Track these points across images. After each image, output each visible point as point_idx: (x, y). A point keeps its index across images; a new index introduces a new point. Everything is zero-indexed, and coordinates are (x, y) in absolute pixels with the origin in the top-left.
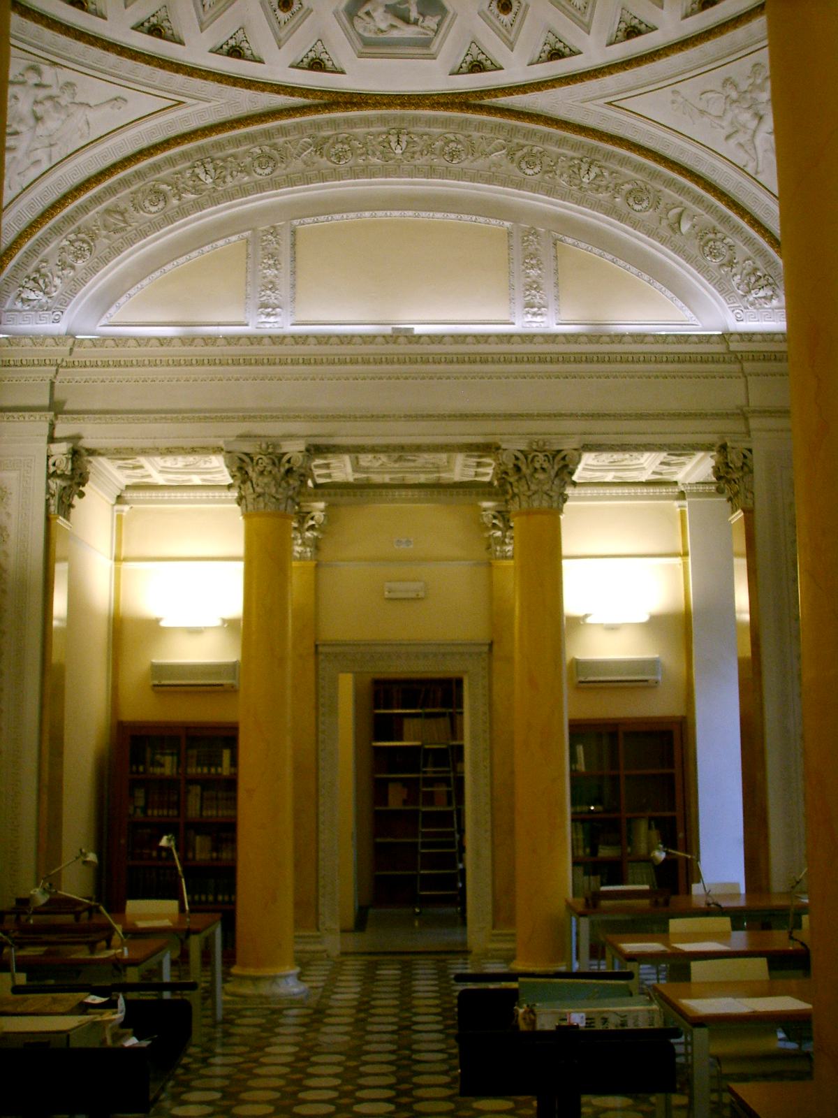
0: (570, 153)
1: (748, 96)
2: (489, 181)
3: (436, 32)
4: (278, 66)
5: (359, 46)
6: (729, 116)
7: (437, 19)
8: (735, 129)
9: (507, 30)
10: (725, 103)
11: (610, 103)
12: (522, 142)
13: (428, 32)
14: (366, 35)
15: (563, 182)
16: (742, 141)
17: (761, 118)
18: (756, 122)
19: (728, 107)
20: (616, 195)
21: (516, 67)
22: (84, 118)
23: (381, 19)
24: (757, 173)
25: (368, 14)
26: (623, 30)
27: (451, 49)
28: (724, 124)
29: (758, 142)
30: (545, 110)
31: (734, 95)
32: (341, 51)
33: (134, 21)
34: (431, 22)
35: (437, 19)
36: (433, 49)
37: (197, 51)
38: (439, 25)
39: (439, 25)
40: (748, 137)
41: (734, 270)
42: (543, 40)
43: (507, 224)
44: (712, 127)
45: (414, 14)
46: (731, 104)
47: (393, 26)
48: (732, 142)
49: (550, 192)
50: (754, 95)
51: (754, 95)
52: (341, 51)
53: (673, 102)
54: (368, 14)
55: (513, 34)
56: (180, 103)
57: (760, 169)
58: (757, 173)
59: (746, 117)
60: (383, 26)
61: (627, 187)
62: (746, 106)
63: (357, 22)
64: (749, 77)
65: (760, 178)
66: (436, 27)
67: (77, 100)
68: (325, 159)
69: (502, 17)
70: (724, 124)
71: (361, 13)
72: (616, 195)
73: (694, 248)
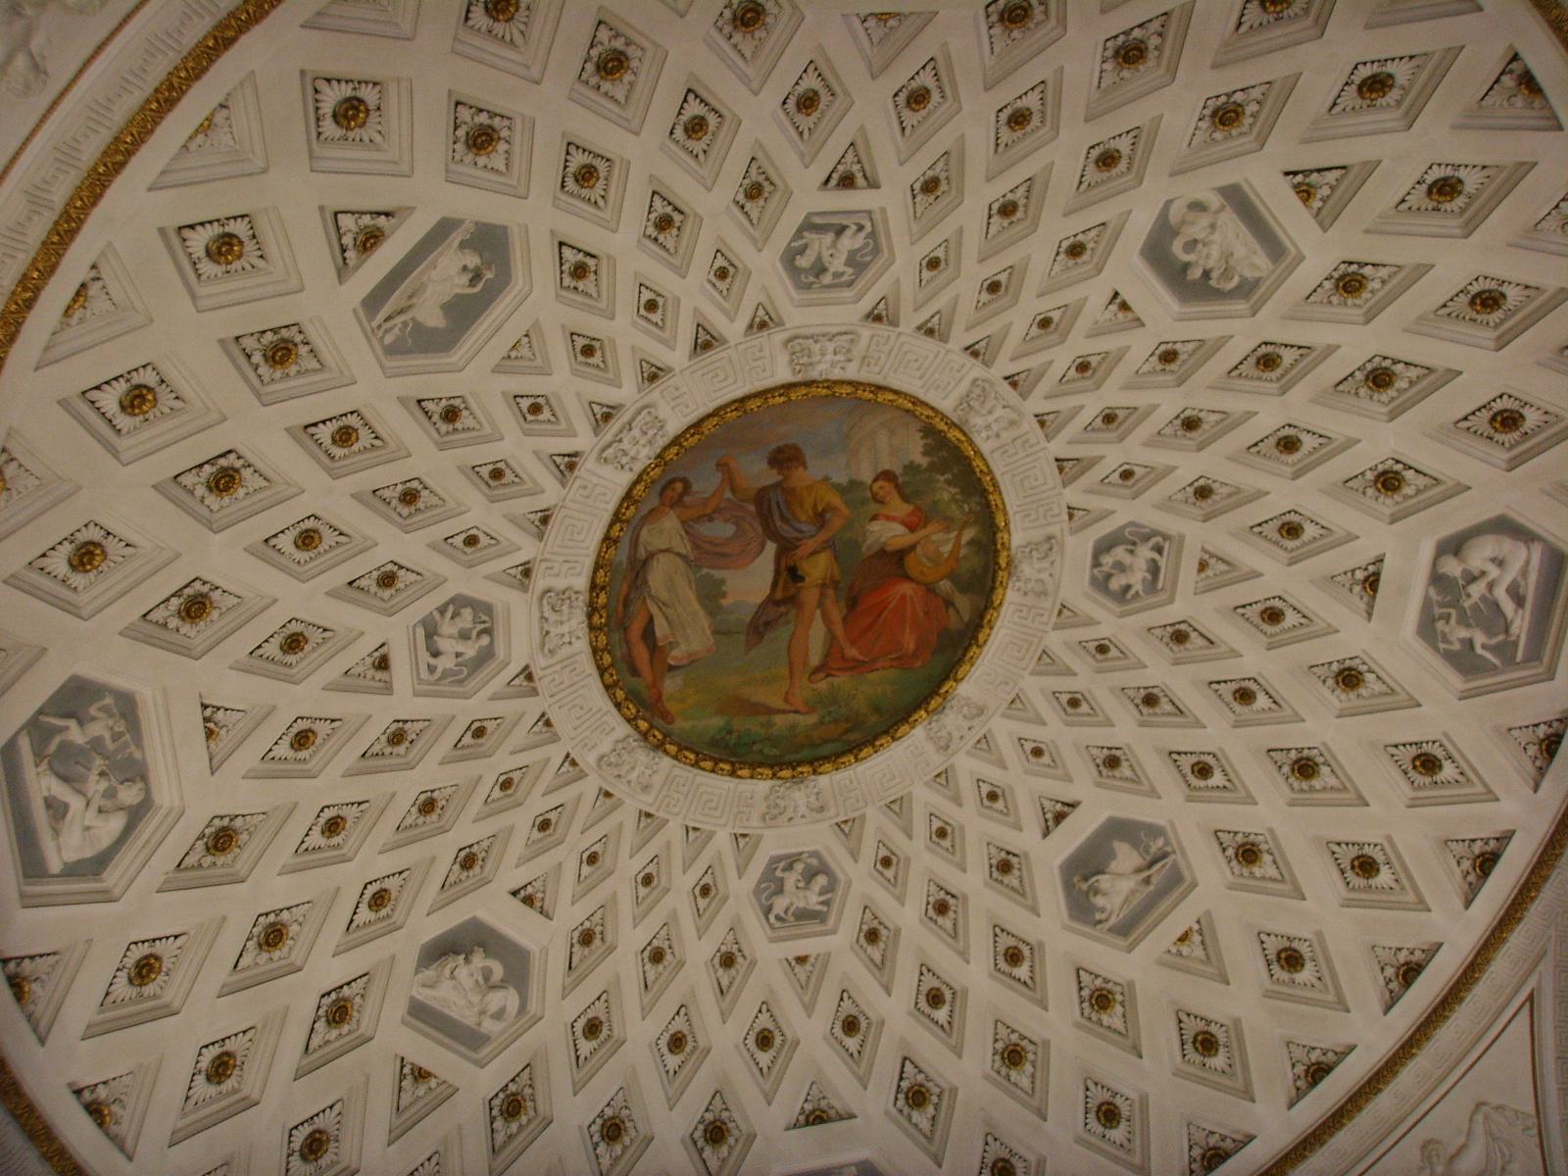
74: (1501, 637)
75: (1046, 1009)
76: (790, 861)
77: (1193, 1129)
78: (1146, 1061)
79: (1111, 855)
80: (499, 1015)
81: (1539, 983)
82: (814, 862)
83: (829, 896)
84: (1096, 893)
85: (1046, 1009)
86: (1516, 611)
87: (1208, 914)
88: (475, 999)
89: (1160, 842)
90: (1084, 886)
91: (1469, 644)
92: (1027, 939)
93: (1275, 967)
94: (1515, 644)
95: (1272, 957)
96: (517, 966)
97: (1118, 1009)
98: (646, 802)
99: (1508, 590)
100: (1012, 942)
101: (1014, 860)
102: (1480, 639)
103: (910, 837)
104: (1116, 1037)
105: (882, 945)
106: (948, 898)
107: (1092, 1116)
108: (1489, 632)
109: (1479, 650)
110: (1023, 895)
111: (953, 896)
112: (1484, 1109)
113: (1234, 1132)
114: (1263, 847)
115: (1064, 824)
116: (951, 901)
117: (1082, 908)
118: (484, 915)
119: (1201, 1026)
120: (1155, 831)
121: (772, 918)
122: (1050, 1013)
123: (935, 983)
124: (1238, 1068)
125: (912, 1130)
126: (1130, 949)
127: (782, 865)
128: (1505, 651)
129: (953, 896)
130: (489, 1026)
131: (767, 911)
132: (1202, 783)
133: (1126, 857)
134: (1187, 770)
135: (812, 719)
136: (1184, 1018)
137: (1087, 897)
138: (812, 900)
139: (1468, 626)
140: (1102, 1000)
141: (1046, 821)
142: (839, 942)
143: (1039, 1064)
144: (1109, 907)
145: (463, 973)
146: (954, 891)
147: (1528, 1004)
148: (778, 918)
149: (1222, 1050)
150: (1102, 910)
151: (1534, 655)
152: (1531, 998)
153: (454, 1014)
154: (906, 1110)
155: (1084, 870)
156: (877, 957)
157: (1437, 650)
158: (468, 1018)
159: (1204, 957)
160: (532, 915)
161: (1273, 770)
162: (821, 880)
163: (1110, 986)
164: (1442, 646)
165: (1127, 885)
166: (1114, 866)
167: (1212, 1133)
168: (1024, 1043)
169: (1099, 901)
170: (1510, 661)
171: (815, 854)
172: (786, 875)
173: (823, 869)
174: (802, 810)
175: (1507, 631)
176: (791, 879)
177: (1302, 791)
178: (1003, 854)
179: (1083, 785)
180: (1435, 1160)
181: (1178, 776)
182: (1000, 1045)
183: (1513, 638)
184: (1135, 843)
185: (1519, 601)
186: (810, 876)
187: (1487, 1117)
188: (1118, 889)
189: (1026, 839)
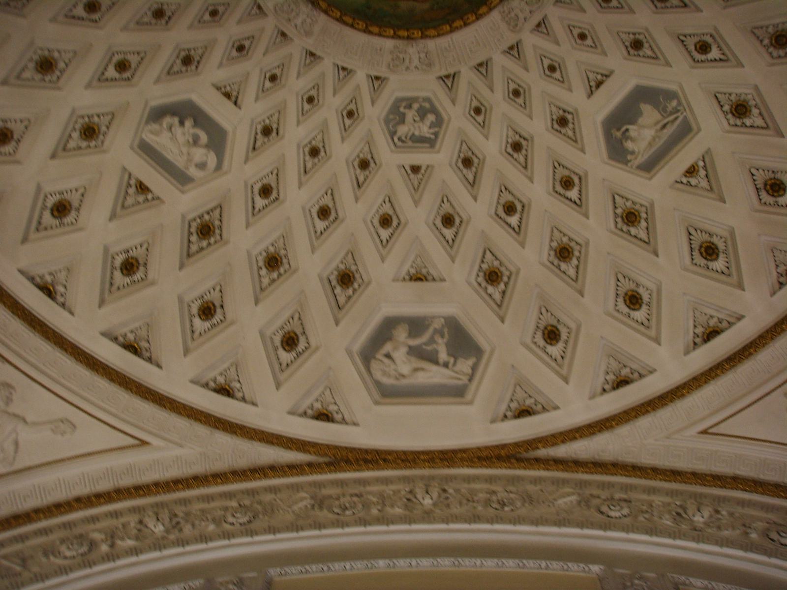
0: (668, 499)
2: (560, 523)
4: (274, 408)
5: (377, 396)
7: (471, 362)
9: (558, 365)
11: (705, 432)
12: (595, 492)
13: (461, 377)
14: (385, 380)
15: (667, 521)
20: (749, 531)
22: (14, 436)
23: (403, 363)
25: (388, 356)
26: (700, 335)
27: (490, 390)
30: (620, 459)
32: (355, 396)
33: (104, 326)
34: (465, 365)
35: (471, 362)
36: (469, 396)
37: (176, 378)
38: (474, 368)
39: (474, 368)
42: (603, 368)
43: (596, 568)
45: (443, 356)
47: (416, 370)
49: (652, 531)
52: (355, 396)
54: (388, 356)
55: (565, 367)
56: (144, 443)
60: (405, 369)
61: (760, 525)
63: (375, 366)
66: (470, 371)
67: (12, 409)
68: (325, 511)
69: (550, 349)
71: (379, 356)
72: (749, 531)
75: (588, 218)
76: (409, 102)
77: (698, 314)
78: (661, 260)
79: (640, 113)
80: (202, 166)
82: (427, 105)
83: (436, 129)
84: (628, 138)
85: (588, 218)
87: (708, 151)
88: (185, 150)
89: (674, 103)
90: (619, 134)
92: (577, 171)
93: (764, 194)
95: (760, 185)
96: (217, 140)
97: (643, 224)
98: (310, 43)
100: (566, 173)
101: (569, 117)
103: (492, 91)
104: (642, 244)
105: (474, 169)
106: (522, 140)
110: (576, 141)
111: (525, 139)
113: (730, 316)
114: (752, 103)
115: (602, 87)
116: (524, 143)
117: (618, 152)
118: (195, 98)
119: (706, 237)
120: (670, 95)
121: (396, 139)
122: (592, 221)
123: (510, 198)
124: (733, 269)
125: (487, 298)
126: (650, 179)
127: (404, 104)
129: (525, 139)
130: (193, 171)
131: (392, 134)
132: (703, 57)
133: (649, 114)
134: (692, 48)
135: (426, 6)
136: (692, 231)
137: (622, 143)
138: (425, 130)
140: (631, 218)
141: (591, 87)
142: (441, 159)
143: (582, 260)
144: (636, 150)
145: (178, 131)
146: (526, 136)
148: (400, 139)
149: (721, 255)
150: (633, 153)
153: (170, 157)
154: (484, 284)
155: (619, 122)
156: (471, 177)
158: (179, 162)
159: (708, 188)
160: (229, 104)
161: (757, 44)
162: (431, 118)
163: (637, 207)
165: (648, 134)
166: (640, 121)
167: (712, 317)
168: (573, 244)
169: (629, 145)
171: (428, 100)
172: (407, 111)
173: (434, 110)
174: (416, 62)
176: (410, 115)
178: (561, 112)
179: (615, 59)
181: (686, 54)
182: (554, 244)
184: (656, 105)
186: (422, 114)
188: (644, 135)
189: (575, 98)
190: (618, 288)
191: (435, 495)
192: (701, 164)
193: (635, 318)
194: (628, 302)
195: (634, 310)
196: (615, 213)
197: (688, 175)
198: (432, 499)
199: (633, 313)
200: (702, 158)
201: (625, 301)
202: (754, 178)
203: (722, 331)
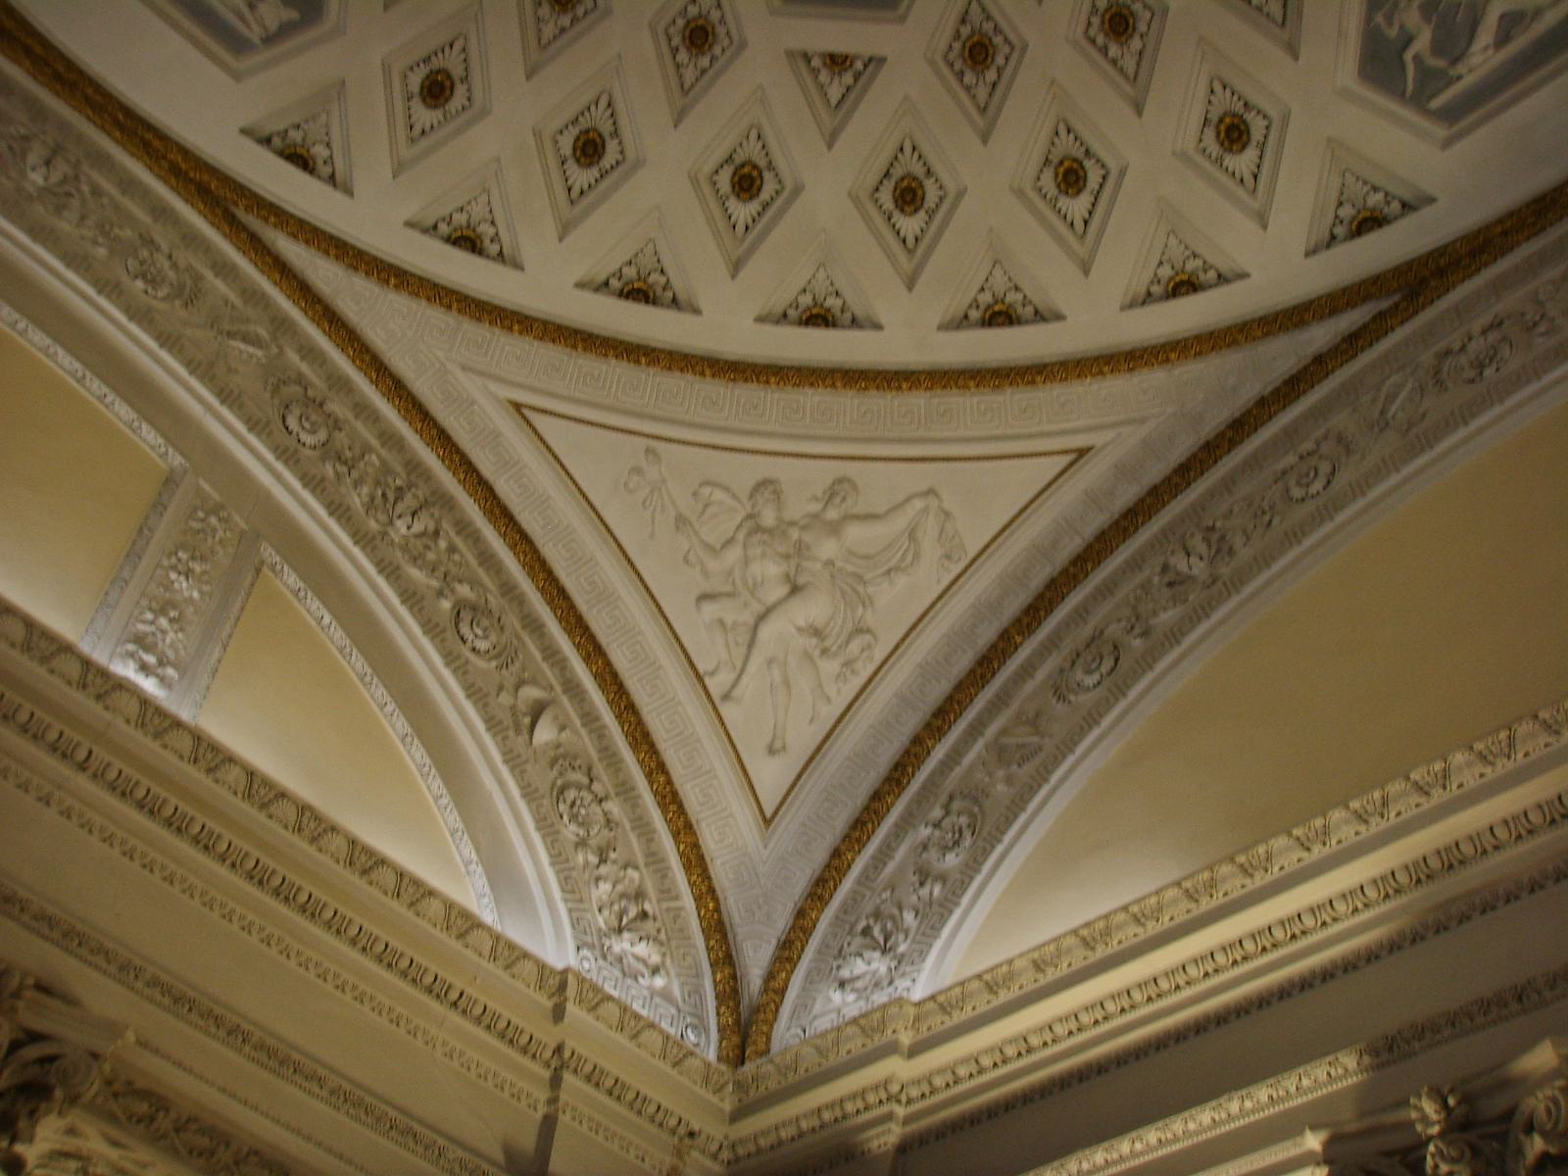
1: (795, 534)
3: (269, 40)
6: (734, 554)
8: (728, 588)
10: (738, 528)
13: (254, 26)
16: (729, 619)
17: (795, 589)
18: (784, 590)
19: (741, 536)
21: (377, 212)
24: (726, 697)
27: (276, 88)
28: (713, 565)
29: (766, 632)
31: (769, 518)
35: (292, 14)
39: (286, 30)
40: (748, 617)
41: (603, 870)
44: (686, 560)
46: (749, 534)
48: (710, 610)
50: (808, 538)
51: (808, 538)
53: (637, 471)
57: (736, 693)
58: (726, 697)
59: (770, 570)
62: (781, 550)
64: (815, 499)
65: (726, 710)
70: (713, 565)
73: (543, 778)
74: (1439, 63)
81: (1104, 447)
86: (1486, 48)
91: (1408, 40)
93: (888, 187)
94: (1450, 82)
99: (1502, 17)
102: (1422, 43)
107: (574, 131)
108: (1437, 48)
109: (1408, 56)
112: (934, 503)
128: (1431, 80)
139: (1427, 19)
147: (1072, 456)
151: (1450, 115)
152: (1082, 453)
157: (1369, 18)
164: (1379, 19)
170: (1418, 101)
175: (1455, 61)
177: (1093, 41)
180: (837, 500)
183: (1453, 72)
185: (1502, 39)
187: (926, 510)
190: (586, 114)
191: (56, 177)
192: (859, 65)
193: (568, 173)
194: (580, 144)
195: (578, 161)
196: (686, 8)
197: (828, 61)
198: (46, 179)
199: (571, 165)
200: (866, 60)
201: (577, 139)
202: (900, 156)
203: (654, 303)
